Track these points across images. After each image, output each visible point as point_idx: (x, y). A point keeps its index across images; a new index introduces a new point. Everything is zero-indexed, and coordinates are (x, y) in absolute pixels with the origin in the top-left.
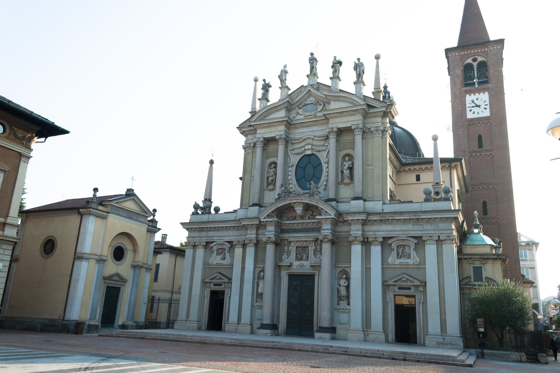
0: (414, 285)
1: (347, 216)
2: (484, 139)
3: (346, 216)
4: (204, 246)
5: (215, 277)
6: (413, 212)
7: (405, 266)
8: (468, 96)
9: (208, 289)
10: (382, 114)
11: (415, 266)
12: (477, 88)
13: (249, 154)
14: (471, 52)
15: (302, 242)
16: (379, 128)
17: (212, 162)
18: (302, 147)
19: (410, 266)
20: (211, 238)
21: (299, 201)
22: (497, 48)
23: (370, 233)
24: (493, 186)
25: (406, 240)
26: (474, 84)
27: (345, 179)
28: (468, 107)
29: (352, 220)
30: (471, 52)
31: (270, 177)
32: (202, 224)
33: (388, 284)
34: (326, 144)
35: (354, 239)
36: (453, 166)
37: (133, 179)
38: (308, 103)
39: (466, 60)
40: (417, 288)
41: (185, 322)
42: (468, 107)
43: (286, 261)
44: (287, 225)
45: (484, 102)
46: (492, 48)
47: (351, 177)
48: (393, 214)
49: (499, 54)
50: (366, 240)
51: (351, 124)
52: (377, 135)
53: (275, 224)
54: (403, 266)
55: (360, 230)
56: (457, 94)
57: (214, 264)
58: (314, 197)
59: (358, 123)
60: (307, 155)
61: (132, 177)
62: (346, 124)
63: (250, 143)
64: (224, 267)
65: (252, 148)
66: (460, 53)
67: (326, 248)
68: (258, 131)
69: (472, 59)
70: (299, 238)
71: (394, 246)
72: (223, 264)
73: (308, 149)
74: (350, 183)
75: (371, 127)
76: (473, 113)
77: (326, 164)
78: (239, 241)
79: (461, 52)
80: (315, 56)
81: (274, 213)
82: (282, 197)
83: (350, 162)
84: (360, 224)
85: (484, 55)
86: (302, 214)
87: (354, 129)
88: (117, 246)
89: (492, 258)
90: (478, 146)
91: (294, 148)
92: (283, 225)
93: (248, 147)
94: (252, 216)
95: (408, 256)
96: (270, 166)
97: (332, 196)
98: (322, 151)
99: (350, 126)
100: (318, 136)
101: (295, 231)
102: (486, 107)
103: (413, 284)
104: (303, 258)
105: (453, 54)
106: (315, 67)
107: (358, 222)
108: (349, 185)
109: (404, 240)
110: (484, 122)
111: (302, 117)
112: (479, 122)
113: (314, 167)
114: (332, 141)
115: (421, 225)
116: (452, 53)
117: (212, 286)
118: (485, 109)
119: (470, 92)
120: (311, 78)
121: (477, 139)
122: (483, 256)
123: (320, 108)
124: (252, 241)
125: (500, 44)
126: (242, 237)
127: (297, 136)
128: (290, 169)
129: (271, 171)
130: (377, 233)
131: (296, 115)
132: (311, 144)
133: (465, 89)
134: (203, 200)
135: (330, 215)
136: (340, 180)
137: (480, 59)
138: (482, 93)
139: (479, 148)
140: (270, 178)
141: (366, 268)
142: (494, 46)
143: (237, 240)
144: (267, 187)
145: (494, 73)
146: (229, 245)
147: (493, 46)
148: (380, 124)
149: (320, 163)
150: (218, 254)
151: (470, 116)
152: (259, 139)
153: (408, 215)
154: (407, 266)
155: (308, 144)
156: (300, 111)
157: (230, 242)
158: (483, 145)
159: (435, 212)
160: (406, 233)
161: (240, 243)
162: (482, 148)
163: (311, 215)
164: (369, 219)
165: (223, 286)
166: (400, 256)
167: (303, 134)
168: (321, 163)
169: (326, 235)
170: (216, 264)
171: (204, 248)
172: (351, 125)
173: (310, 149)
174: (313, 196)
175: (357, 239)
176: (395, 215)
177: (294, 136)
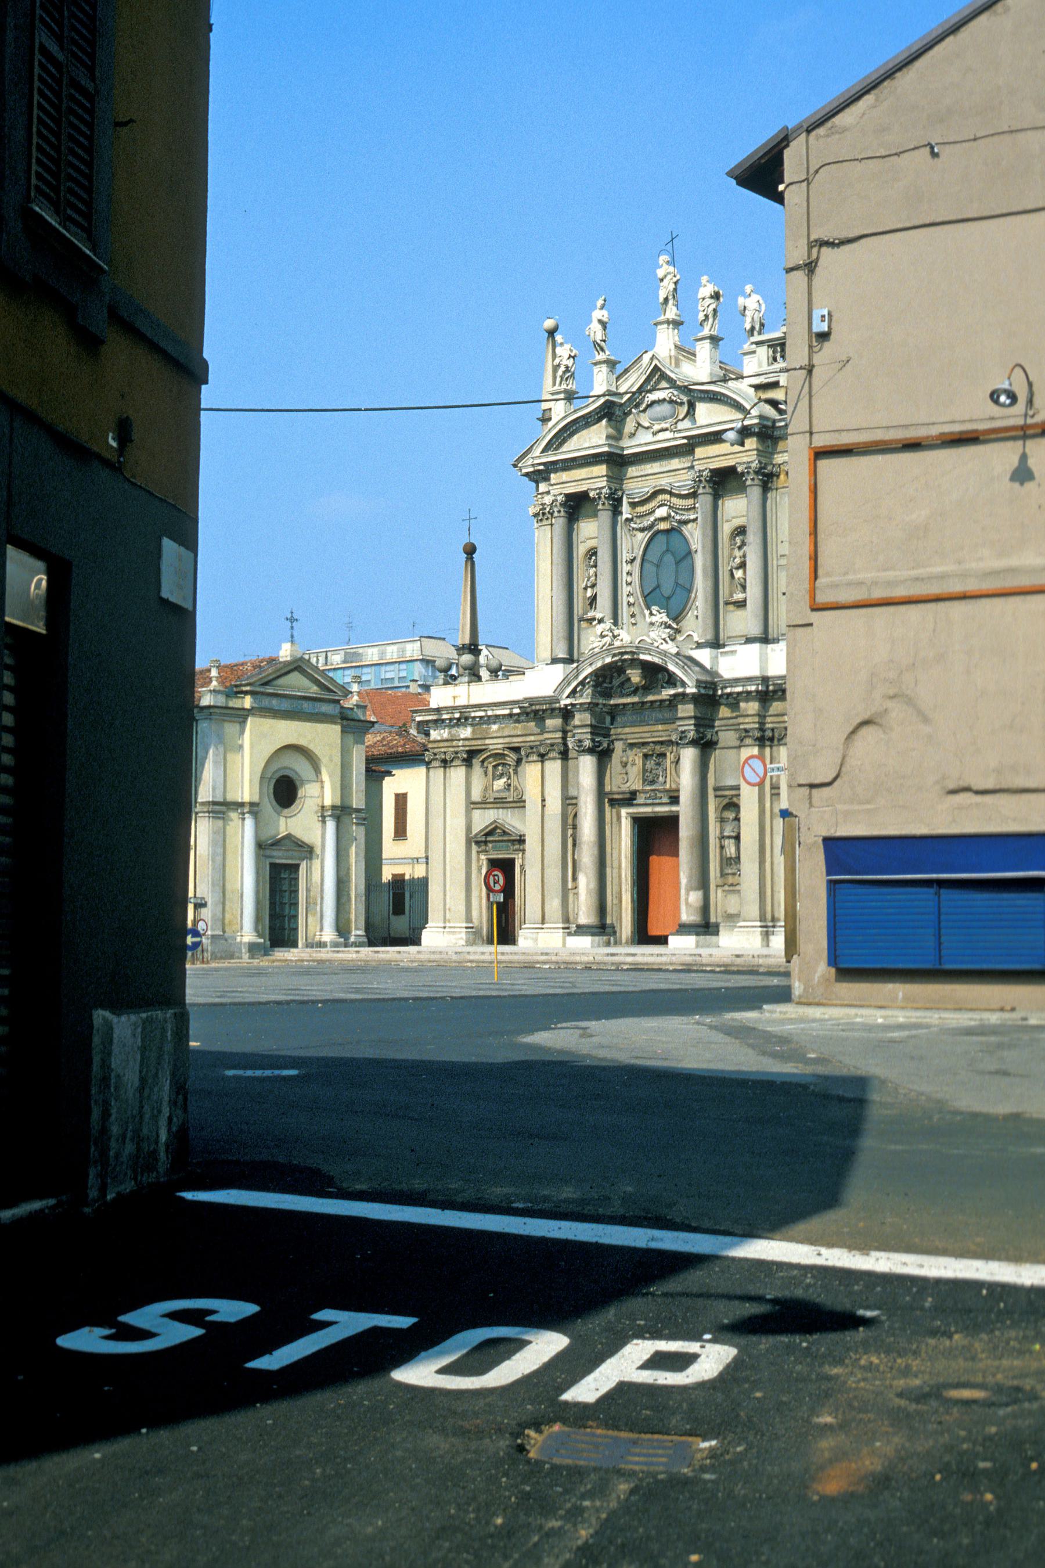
4: (464, 760)
17: (470, 551)
20: (479, 742)
31: (589, 590)
35: (744, 734)
37: (292, 620)
41: (442, 930)
44: (621, 707)
61: (289, 616)
67: (689, 756)
72: (508, 800)
73: (663, 519)
86: (643, 682)
87: (743, 474)
88: (277, 775)
99: (733, 464)
104: (658, 778)
106: (670, 297)
114: (704, 502)
141: (772, 795)
143: (528, 744)
157: (516, 750)
169: (683, 732)
170: (492, 800)
171: (466, 766)
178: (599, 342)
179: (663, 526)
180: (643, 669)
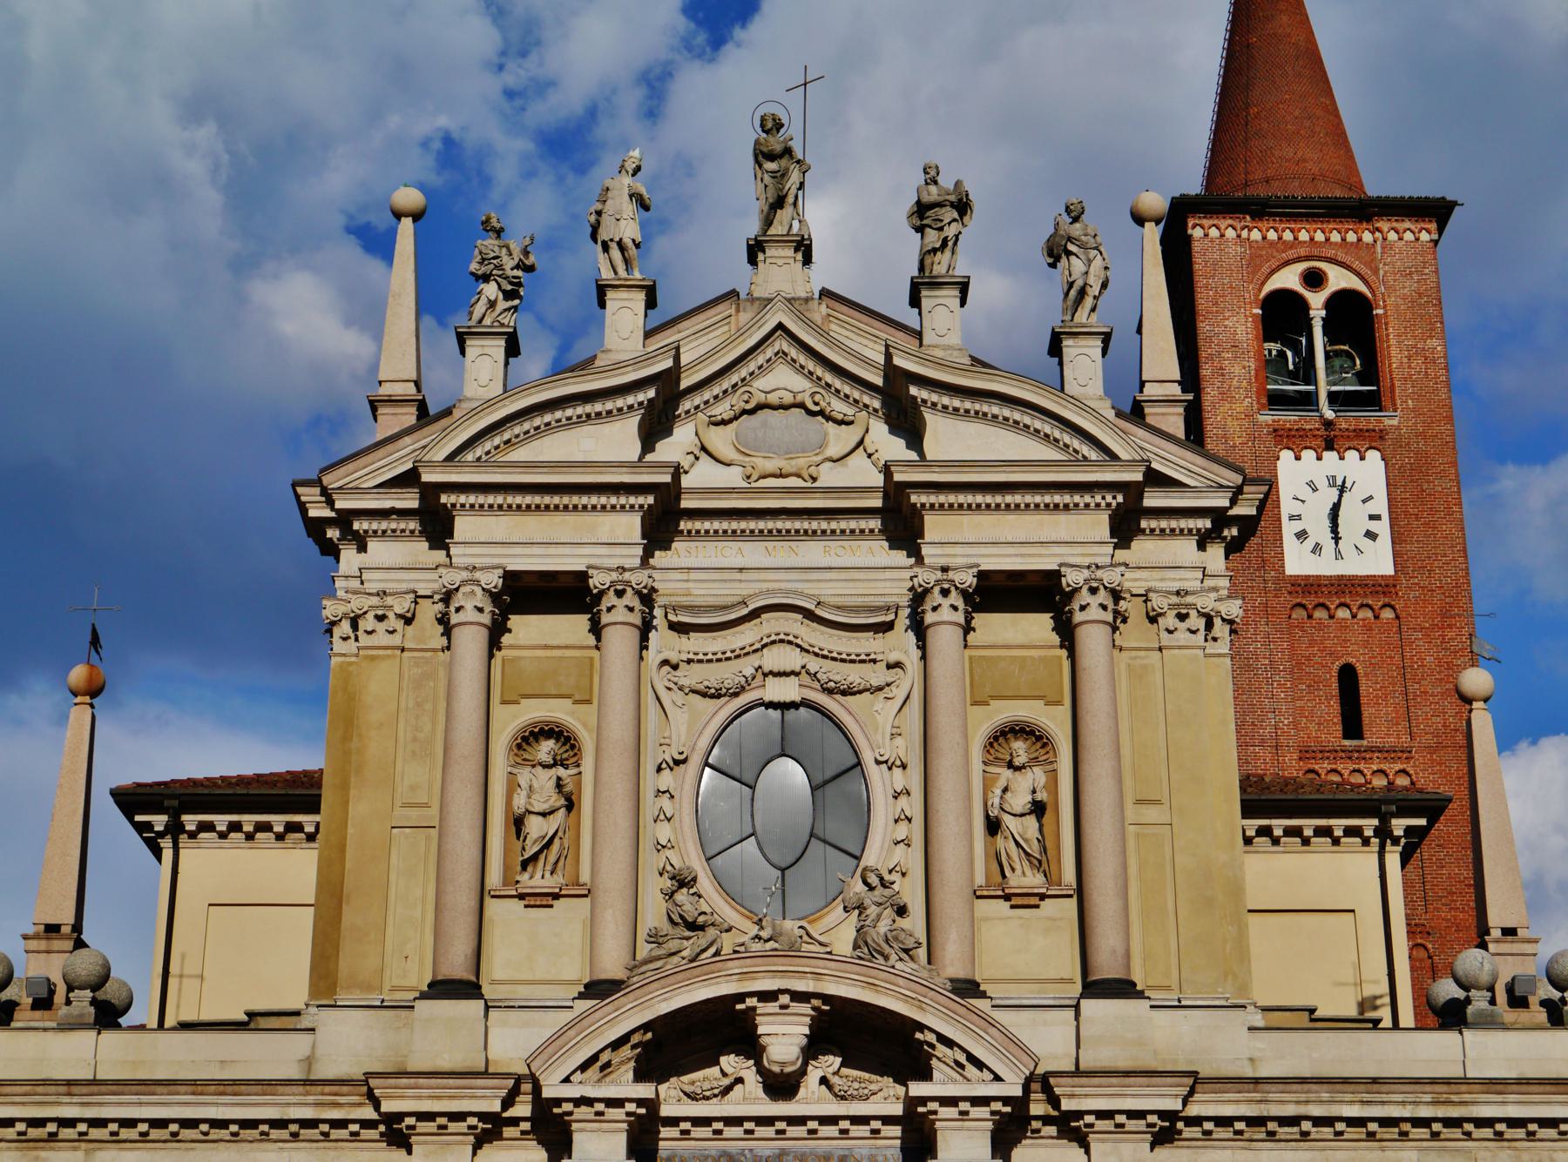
1: (1078, 1090)
2: (1365, 687)
6: (1433, 1081)
8: (1286, 456)
10: (1208, 524)
12: (1328, 424)
13: (373, 658)
14: (1296, 238)
16: (1189, 599)
18: (738, 657)
22: (1417, 239)
24: (1419, 941)
26: (1307, 401)
27: (1013, 870)
28: (1292, 518)
30: (1296, 238)
32: (66, 1099)
34: (893, 657)
36: (1398, 832)
38: (773, 399)
42: (1292, 518)
45: (1364, 501)
46: (1392, 236)
47: (1042, 862)
48: (1330, 1087)
49: (1427, 271)
51: (1059, 561)
52: (1182, 637)
53: (630, 1123)
56: (1238, 442)
58: (893, 967)
59: (1100, 561)
62: (1022, 555)
63: (383, 594)
65: (399, 625)
66: (1245, 234)
68: (464, 526)
69: (1302, 274)
74: (1043, 897)
75: (1149, 590)
76: (1313, 551)
77: (897, 772)
79: (1250, 230)
80: (793, 132)
81: (626, 1051)
83: (1037, 776)
84: (1143, 1140)
85: (1356, 265)
90: (1340, 727)
91: (685, 657)
93: (370, 616)
94: (445, 1064)
96: (519, 746)
97: (953, 965)
98: (860, 692)
102: (1374, 526)
105: (1214, 232)
106: (790, 199)
107: (1132, 1125)
108: (1037, 906)
110: (1368, 606)
111: (732, 477)
112: (1343, 600)
113: (819, 779)
115: (1468, 1151)
116: (1206, 222)
118: (1371, 535)
119: (1293, 440)
120: (780, 262)
121: (1335, 685)
123: (840, 440)
125: (1430, 221)
127: (704, 591)
128: (667, 780)
129: (544, 780)
131: (691, 457)
132: (799, 641)
133: (1274, 421)
134: (31, 930)
135: (997, 1078)
136: (980, 879)
137: (1338, 279)
138: (1352, 455)
139: (1346, 737)
140: (536, 828)
142: (1407, 224)
144: (508, 880)
145: (1405, 360)
147: (1401, 226)
148: (1191, 581)
149: (853, 761)
151: (1298, 561)
152: (478, 575)
153: (1411, 1097)
155: (773, 642)
156: (720, 440)
158: (1366, 721)
159: (1548, 1088)
162: (1361, 737)
163: (834, 1074)
164: (1193, 1110)
167: (738, 576)
168: (859, 764)
172: (1061, 565)
174: (886, 958)
176: (1339, 1097)
177: (685, 585)
178: (628, 242)
179: (786, 690)
180: (811, 1027)
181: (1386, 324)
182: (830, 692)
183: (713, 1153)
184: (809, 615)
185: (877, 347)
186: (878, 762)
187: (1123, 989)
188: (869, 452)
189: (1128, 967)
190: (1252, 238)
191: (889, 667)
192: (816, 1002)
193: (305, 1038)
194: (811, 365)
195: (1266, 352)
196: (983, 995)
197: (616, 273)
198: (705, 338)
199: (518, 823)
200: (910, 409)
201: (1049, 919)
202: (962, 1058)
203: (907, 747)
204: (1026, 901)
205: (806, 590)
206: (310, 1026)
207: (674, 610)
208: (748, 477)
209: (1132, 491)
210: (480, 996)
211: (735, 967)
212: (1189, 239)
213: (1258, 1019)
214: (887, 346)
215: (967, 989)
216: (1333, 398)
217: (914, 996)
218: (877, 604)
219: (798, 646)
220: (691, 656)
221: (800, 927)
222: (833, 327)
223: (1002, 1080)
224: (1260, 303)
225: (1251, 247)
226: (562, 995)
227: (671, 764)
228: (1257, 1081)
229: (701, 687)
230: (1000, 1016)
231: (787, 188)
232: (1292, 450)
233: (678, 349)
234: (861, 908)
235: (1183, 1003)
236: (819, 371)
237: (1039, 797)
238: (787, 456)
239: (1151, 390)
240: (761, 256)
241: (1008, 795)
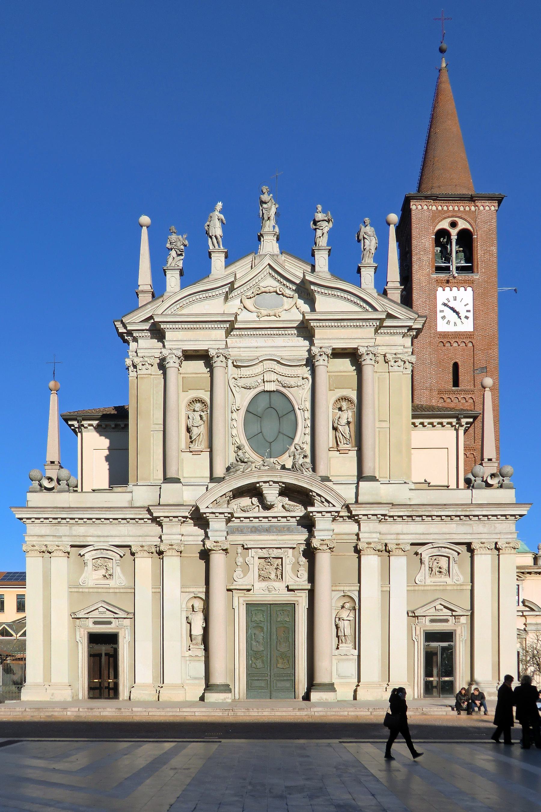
0: (455, 616)
3: (355, 509)
5: (97, 609)
7: (441, 588)
9: (82, 630)
11: (455, 588)
14: (448, 209)
15: (271, 550)
19: (448, 588)
21: (276, 480)
23: (389, 537)
25: (445, 548)
29: (364, 515)
30: (448, 209)
33: (416, 615)
34: (305, 376)
39: (439, 222)
40: (458, 619)
43: (242, 582)
50: (384, 548)
54: (438, 588)
55: (376, 532)
57: (89, 586)
60: (267, 391)
64: (111, 591)
70: (263, 542)
71: (426, 557)
72: (111, 586)
74: (349, 450)
78: (142, 546)
82: (241, 470)
89: (535, 572)
92: (234, 519)
95: (445, 572)
100: (286, 358)
101: (255, 530)
103: (454, 613)
105: (420, 207)
109: (441, 547)
116: (417, 203)
117: (91, 625)
122: (523, 569)
124: (174, 547)
126: (148, 537)
127: (245, 354)
128: (235, 415)
129: (197, 415)
130: (401, 537)
132: (275, 371)
135: (334, 506)
137: (462, 225)
140: (195, 431)
143: (141, 544)
146: (121, 551)
150: (96, 568)
154: (444, 588)
160: (448, 536)
161: (145, 548)
164: (391, 514)
165: (113, 626)
166: (433, 572)
167: (256, 350)
168: (294, 410)
170: (94, 586)
173: (274, 381)
175: (372, 546)
181: (477, 241)
182: (284, 387)
183: (250, 527)
184: (278, 362)
185: (300, 271)
186: (299, 409)
187: (373, 479)
188: (298, 307)
189: (374, 472)
190: (433, 209)
191: (303, 379)
192: (280, 484)
193: (131, 494)
194: (279, 278)
195: (436, 251)
196: (330, 481)
197: (215, 247)
198: (244, 268)
199: (188, 430)
200: (311, 293)
201: (351, 457)
202: (324, 500)
203: (308, 405)
204: (344, 452)
205: (278, 354)
206: (130, 491)
207: (236, 361)
208: (258, 316)
209: (381, 320)
210: (181, 482)
211: (256, 474)
212: (410, 210)
213: (413, 486)
214: (304, 273)
215: (326, 479)
216: (458, 268)
217: (310, 482)
218: (300, 358)
219: (274, 372)
220: (241, 376)
221: (276, 460)
222: (286, 264)
223: (335, 506)
224: (434, 234)
225: (432, 212)
226: (205, 481)
227: (236, 410)
228: (410, 505)
229: (244, 386)
230: (335, 487)
231: (271, 214)
232: (442, 287)
233: (235, 274)
234: (294, 456)
235: (391, 482)
236: (282, 280)
237: (349, 420)
238: (272, 309)
239: (389, 285)
240: (262, 239)
241: (340, 419)
